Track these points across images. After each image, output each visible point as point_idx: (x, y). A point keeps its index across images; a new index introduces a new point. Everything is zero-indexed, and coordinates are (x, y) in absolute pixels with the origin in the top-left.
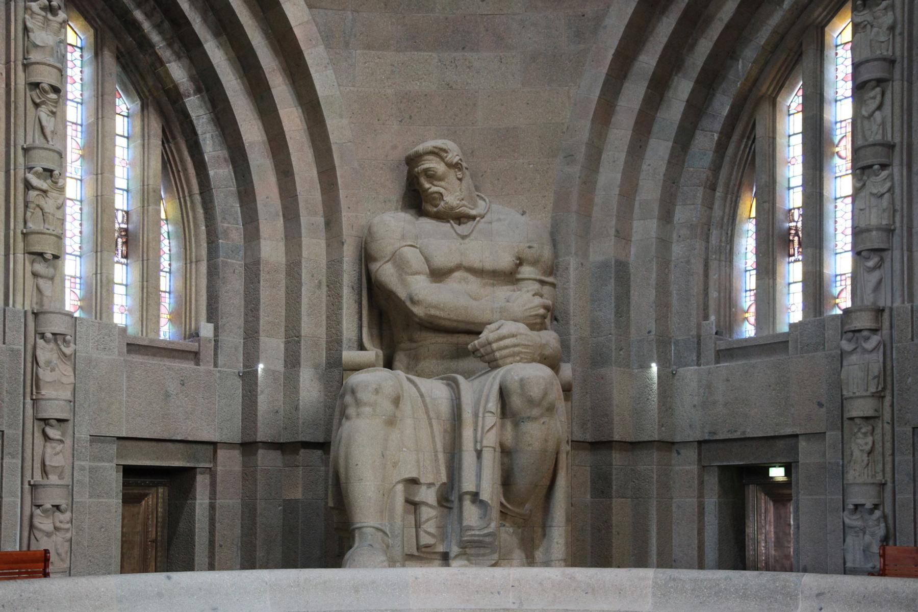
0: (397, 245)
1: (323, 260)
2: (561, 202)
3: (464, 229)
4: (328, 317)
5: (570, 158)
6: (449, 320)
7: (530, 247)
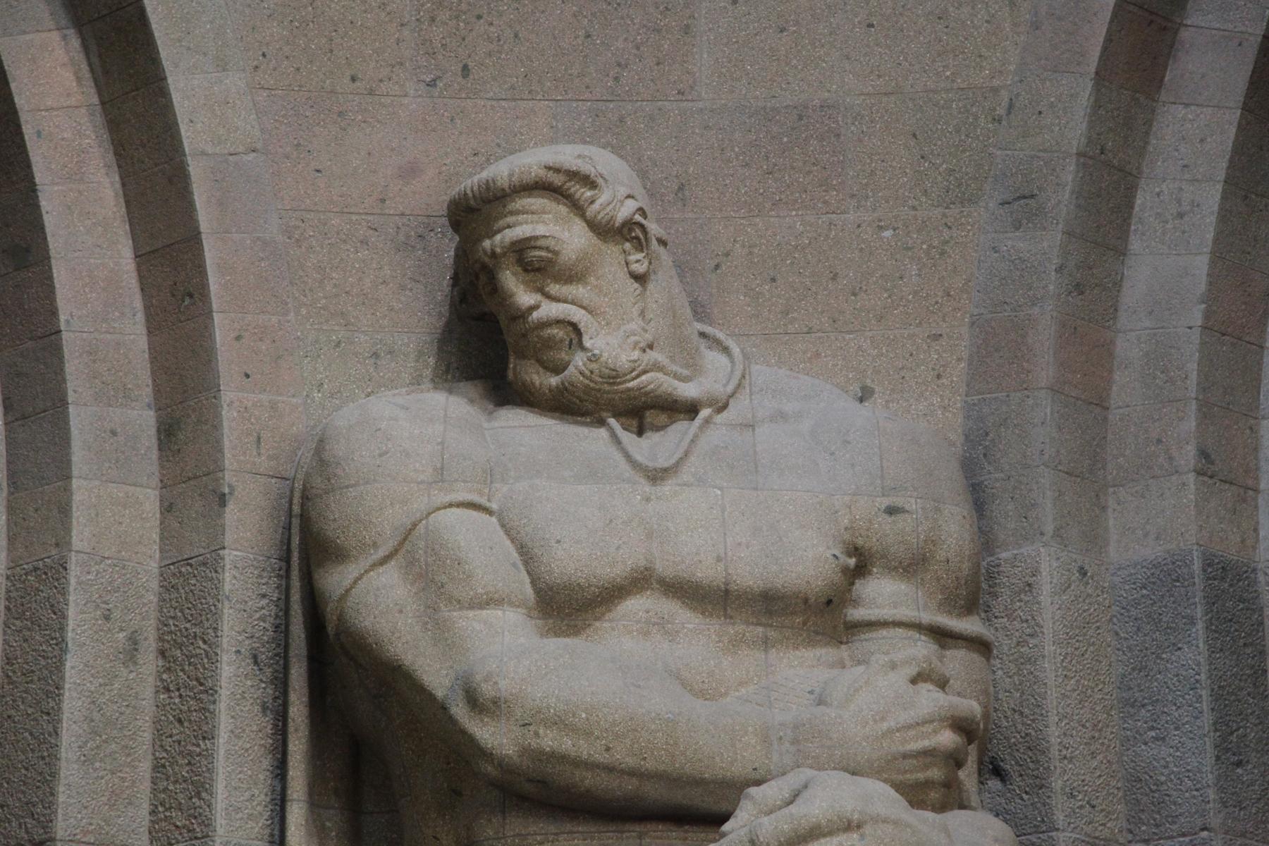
0: (420, 504)
1: (148, 564)
2: (996, 351)
3: (659, 446)
4: (158, 767)
5: (1023, 204)
6: (610, 769)
7: (891, 511)
